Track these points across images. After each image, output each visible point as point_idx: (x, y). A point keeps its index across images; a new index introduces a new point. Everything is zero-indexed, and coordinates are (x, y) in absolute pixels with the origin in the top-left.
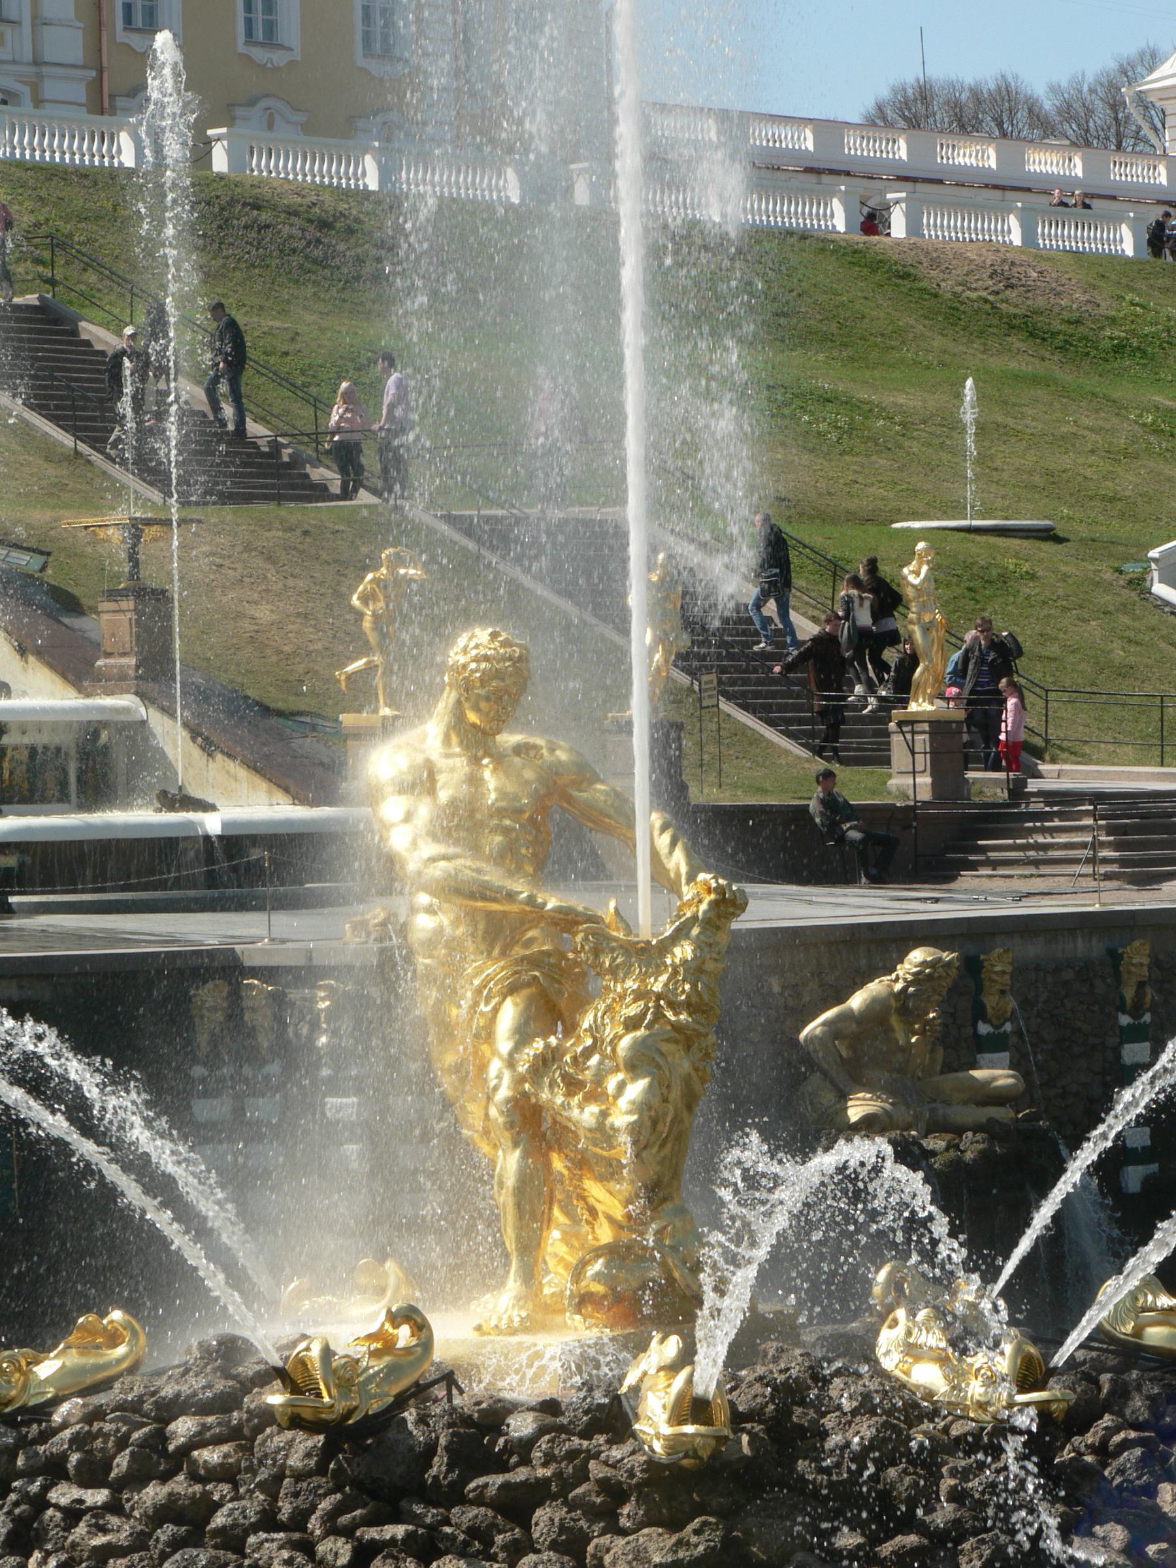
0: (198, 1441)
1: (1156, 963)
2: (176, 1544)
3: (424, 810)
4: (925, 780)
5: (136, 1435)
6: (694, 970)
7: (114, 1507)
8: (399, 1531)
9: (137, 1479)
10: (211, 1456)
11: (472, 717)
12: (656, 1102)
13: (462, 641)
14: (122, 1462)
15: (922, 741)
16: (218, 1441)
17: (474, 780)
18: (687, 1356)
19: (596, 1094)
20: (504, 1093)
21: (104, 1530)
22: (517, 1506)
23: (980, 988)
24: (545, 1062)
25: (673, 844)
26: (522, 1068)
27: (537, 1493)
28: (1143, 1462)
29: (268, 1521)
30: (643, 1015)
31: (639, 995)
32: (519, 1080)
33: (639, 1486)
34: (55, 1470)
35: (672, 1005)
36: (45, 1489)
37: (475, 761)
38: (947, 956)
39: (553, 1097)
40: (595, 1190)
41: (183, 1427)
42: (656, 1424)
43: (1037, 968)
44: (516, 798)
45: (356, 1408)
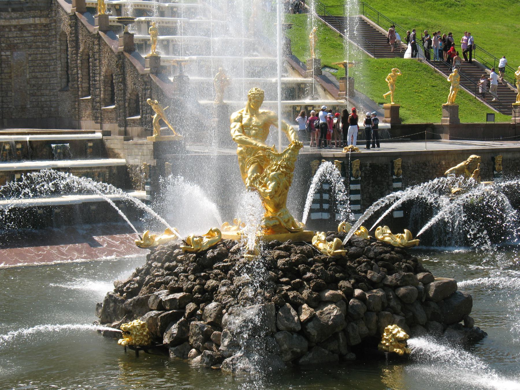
3: (238, 125)
6: (288, 159)
7: (162, 267)
11: (252, 106)
12: (277, 188)
17: (250, 120)
19: (265, 186)
23: (494, 164)
25: (292, 133)
28: (366, 266)
30: (275, 169)
31: (275, 165)
32: (251, 182)
35: (282, 167)
36: (152, 263)
37: (252, 115)
38: (478, 157)
43: (510, 160)
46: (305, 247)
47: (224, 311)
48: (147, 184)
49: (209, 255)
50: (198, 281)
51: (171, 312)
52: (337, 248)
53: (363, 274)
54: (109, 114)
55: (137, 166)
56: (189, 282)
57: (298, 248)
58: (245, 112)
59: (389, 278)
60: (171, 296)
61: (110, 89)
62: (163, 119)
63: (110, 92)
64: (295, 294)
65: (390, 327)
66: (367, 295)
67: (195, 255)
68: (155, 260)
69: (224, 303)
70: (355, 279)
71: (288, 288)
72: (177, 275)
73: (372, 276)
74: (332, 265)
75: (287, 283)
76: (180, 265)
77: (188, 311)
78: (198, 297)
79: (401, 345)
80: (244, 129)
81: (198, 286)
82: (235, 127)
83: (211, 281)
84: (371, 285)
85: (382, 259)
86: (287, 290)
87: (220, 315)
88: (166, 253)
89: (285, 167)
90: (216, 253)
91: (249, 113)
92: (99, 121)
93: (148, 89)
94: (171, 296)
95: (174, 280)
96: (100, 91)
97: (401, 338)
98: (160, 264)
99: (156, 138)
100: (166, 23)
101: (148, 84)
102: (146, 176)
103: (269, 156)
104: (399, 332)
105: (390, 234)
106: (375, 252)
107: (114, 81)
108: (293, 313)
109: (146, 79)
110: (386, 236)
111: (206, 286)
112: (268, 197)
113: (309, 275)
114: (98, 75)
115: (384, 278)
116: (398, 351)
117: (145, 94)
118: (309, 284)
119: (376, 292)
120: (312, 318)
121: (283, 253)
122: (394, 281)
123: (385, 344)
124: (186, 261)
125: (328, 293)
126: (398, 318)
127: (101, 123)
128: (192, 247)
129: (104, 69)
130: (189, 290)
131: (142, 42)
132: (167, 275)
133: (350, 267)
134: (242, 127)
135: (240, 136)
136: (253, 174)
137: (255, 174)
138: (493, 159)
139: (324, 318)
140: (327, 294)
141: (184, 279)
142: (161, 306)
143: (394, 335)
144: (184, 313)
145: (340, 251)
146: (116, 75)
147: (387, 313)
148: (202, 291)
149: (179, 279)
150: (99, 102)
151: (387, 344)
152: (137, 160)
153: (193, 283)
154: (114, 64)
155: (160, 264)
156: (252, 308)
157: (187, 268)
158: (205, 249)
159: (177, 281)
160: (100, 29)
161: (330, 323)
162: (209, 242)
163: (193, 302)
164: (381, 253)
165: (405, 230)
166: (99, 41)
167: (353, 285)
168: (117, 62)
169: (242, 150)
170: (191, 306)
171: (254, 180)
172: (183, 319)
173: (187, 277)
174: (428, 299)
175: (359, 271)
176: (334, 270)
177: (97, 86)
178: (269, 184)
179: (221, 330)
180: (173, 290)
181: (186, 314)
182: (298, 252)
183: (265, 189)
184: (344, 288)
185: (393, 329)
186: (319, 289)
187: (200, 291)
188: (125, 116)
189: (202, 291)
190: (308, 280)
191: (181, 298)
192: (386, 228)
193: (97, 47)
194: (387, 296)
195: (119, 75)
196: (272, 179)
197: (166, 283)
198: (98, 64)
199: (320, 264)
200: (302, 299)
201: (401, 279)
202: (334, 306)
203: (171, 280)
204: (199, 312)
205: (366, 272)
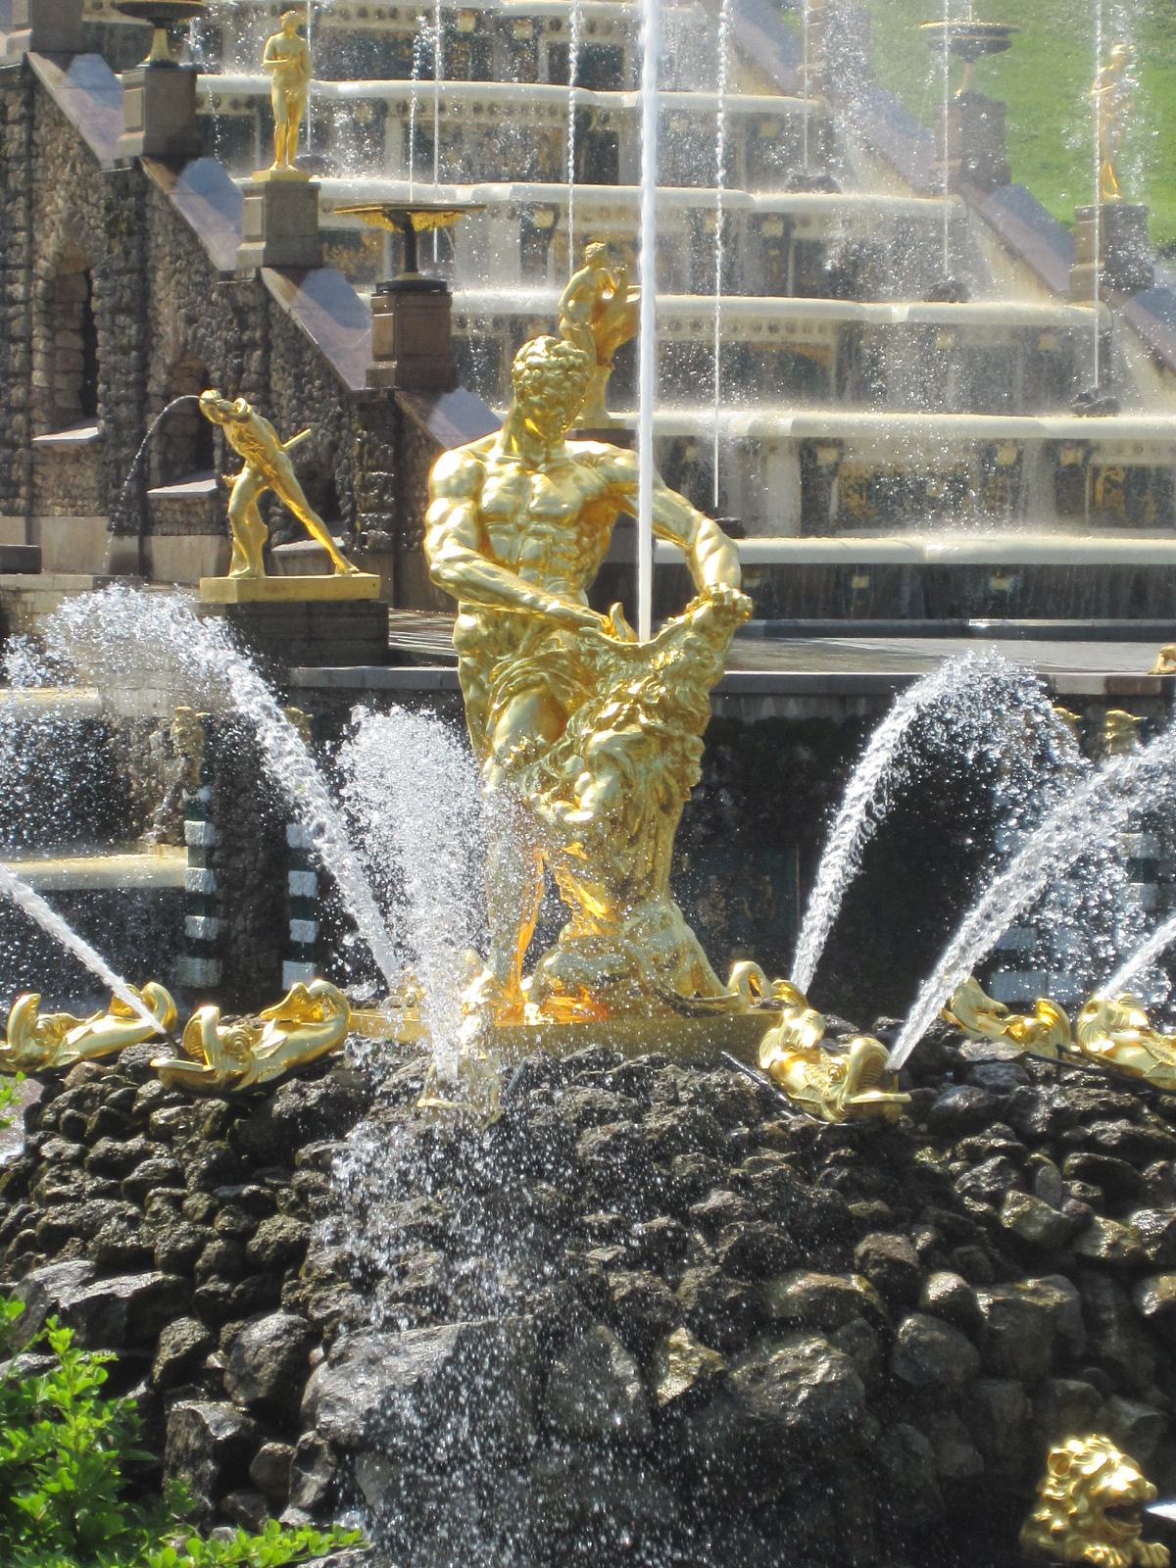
7: (77, 1161)
11: (530, 424)
17: (520, 486)
21: (65, 1181)
25: (712, 551)
28: (998, 1169)
30: (617, 715)
35: (648, 708)
36: (42, 1141)
37: (530, 465)
44: (557, 502)
45: (241, 1077)
46: (715, 1078)
48: (194, 811)
50: (222, 1221)
52: (861, 1083)
53: (982, 1207)
54: (70, 470)
55: (152, 724)
56: (185, 1225)
57: (689, 1081)
58: (497, 452)
59: (1108, 1231)
60: (99, 1288)
61: (78, 342)
62: (280, 493)
63: (78, 360)
64: (640, 1283)
65: (1074, 1446)
66: (984, 1301)
67: (216, 1103)
68: (53, 1129)
69: (317, 1315)
70: (938, 1225)
71: (607, 1257)
72: (137, 1193)
73: (1021, 1217)
74: (839, 1162)
75: (606, 1235)
76: (161, 1149)
77: (166, 1355)
78: (215, 1294)
79: (1120, 1528)
80: (484, 531)
81: (219, 1243)
82: (442, 520)
83: (278, 1219)
84: (1019, 1254)
85: (1091, 1144)
86: (608, 1266)
87: (296, 1368)
88: (103, 1094)
90: (314, 1095)
92: (21, 503)
94: (99, 1288)
95: (122, 1218)
96: (30, 351)
97: (1120, 1498)
98: (73, 1148)
99: (242, 583)
100: (380, 14)
101: (252, 319)
102: (187, 775)
103: (593, 654)
104: (1108, 1467)
105: (1142, 1029)
106: (1056, 1112)
107: (95, 305)
108: (623, 1365)
109: (243, 297)
110: (1129, 1044)
111: (254, 1243)
112: (578, 845)
113: (716, 1199)
114: (21, 274)
115: (1082, 1227)
116: (1100, 1556)
117: (240, 370)
118: (713, 1239)
119: (1034, 1292)
120: (708, 1391)
121: (611, 1100)
122: (1129, 1245)
123: (1046, 1524)
124: (188, 1132)
125: (799, 1285)
126: (1131, 1412)
127: (29, 515)
128: (207, 1068)
129: (49, 245)
130: (181, 1262)
131: (245, 112)
132: (96, 1193)
133: (924, 1171)
134: (480, 518)
135: (466, 559)
136: (514, 739)
137: (526, 741)
139: (767, 1397)
140: (791, 1289)
141: (166, 1209)
143: (1088, 1482)
144: (151, 1361)
145: (873, 1095)
146: (104, 275)
147: (1073, 1384)
148: (238, 1262)
149: (143, 1209)
150: (25, 408)
151: (1058, 1524)
152: (152, 696)
153: (200, 1228)
154: (95, 218)
155: (73, 1148)
156: (429, 1337)
157: (188, 1162)
158: (265, 1076)
159: (134, 1222)
160: (38, 45)
161: (791, 1419)
162: (285, 1046)
163: (193, 1316)
164: (1088, 1117)
166: (29, 103)
167: (924, 1255)
168: (109, 208)
169: (474, 630)
171: (516, 765)
172: (142, 1389)
173: (176, 1202)
175: (967, 1192)
176: (842, 1186)
177: (17, 327)
178: (586, 785)
179: (290, 1437)
180: (112, 1263)
181: (158, 1369)
182: (684, 1096)
183: (565, 810)
184: (877, 1264)
185: (1085, 1457)
186: (755, 1264)
187: (224, 1267)
188: (143, 481)
189: (238, 1262)
190: (712, 1224)
191: (140, 1296)
193: (17, 132)
194: (1089, 1314)
195: (119, 273)
197: (86, 1230)
198: (20, 218)
199: (778, 1156)
200: (673, 1309)
202: (818, 1343)
203: (108, 1217)
204: (214, 1360)
205: (996, 1199)
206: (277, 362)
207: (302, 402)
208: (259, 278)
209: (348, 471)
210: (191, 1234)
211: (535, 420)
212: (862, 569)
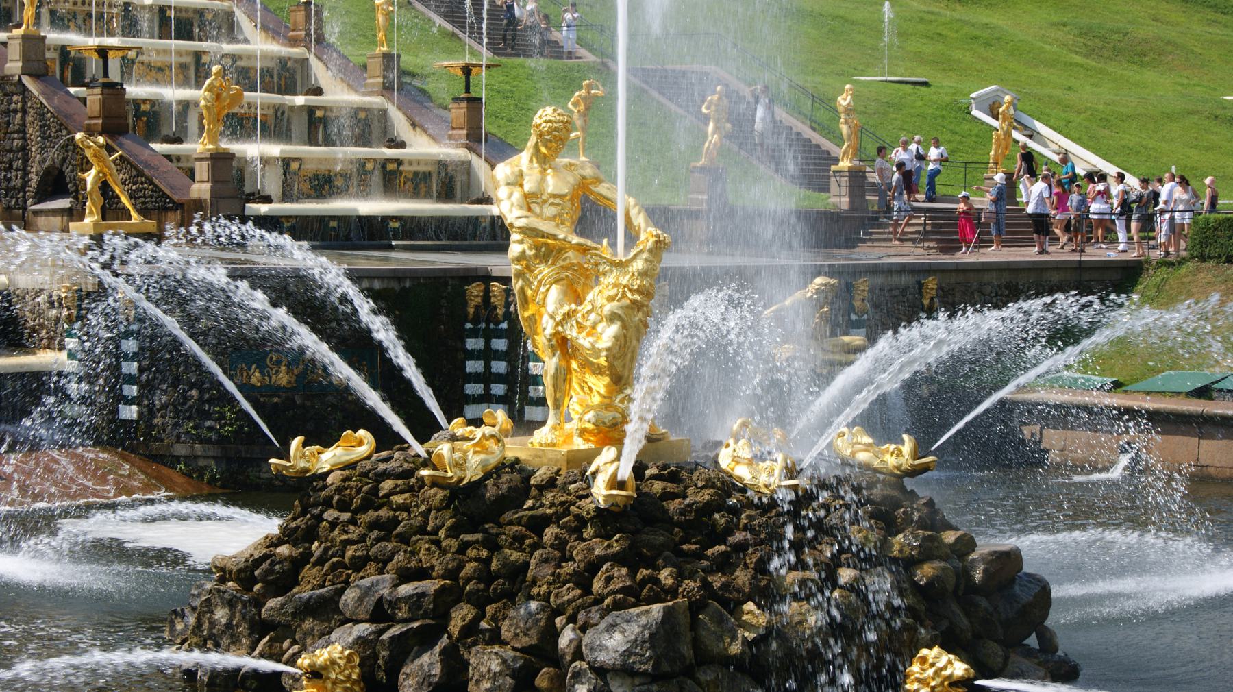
0: (393, 492)
1: (940, 288)
2: (378, 540)
3: (517, 194)
4: (846, 200)
5: (365, 488)
6: (643, 274)
7: (353, 521)
8: (478, 536)
9: (363, 508)
10: (399, 499)
11: (543, 150)
13: (540, 113)
14: (357, 502)
15: (845, 181)
16: (402, 492)
18: (618, 459)
20: (549, 330)
21: (347, 532)
22: (538, 524)
23: (852, 298)
24: (568, 316)
26: (558, 318)
27: (545, 521)
29: (422, 530)
31: (615, 285)
33: (592, 518)
34: (327, 504)
35: (631, 290)
36: (322, 512)
38: (832, 281)
39: (571, 333)
40: (591, 379)
41: (387, 485)
42: (600, 491)
47: (559, 621)
49: (491, 492)
51: (416, 625)
55: (39, 293)
72: (404, 539)
80: (531, 200)
89: (639, 291)
91: (536, 165)
93: (15, 111)
103: (597, 264)
115: (884, 544)
134: (526, 196)
138: (849, 288)
141: (433, 548)
142: (381, 613)
165: (905, 437)
170: (461, 615)
174: (972, 588)
180: (405, 576)
189: (485, 575)
192: (858, 431)
196: (612, 318)
201: (919, 546)
204: (484, 625)
206: (29, 119)
207: (44, 138)
208: (20, 80)
209: (72, 171)
210: (454, 559)
211: (546, 147)
212: (333, 218)
